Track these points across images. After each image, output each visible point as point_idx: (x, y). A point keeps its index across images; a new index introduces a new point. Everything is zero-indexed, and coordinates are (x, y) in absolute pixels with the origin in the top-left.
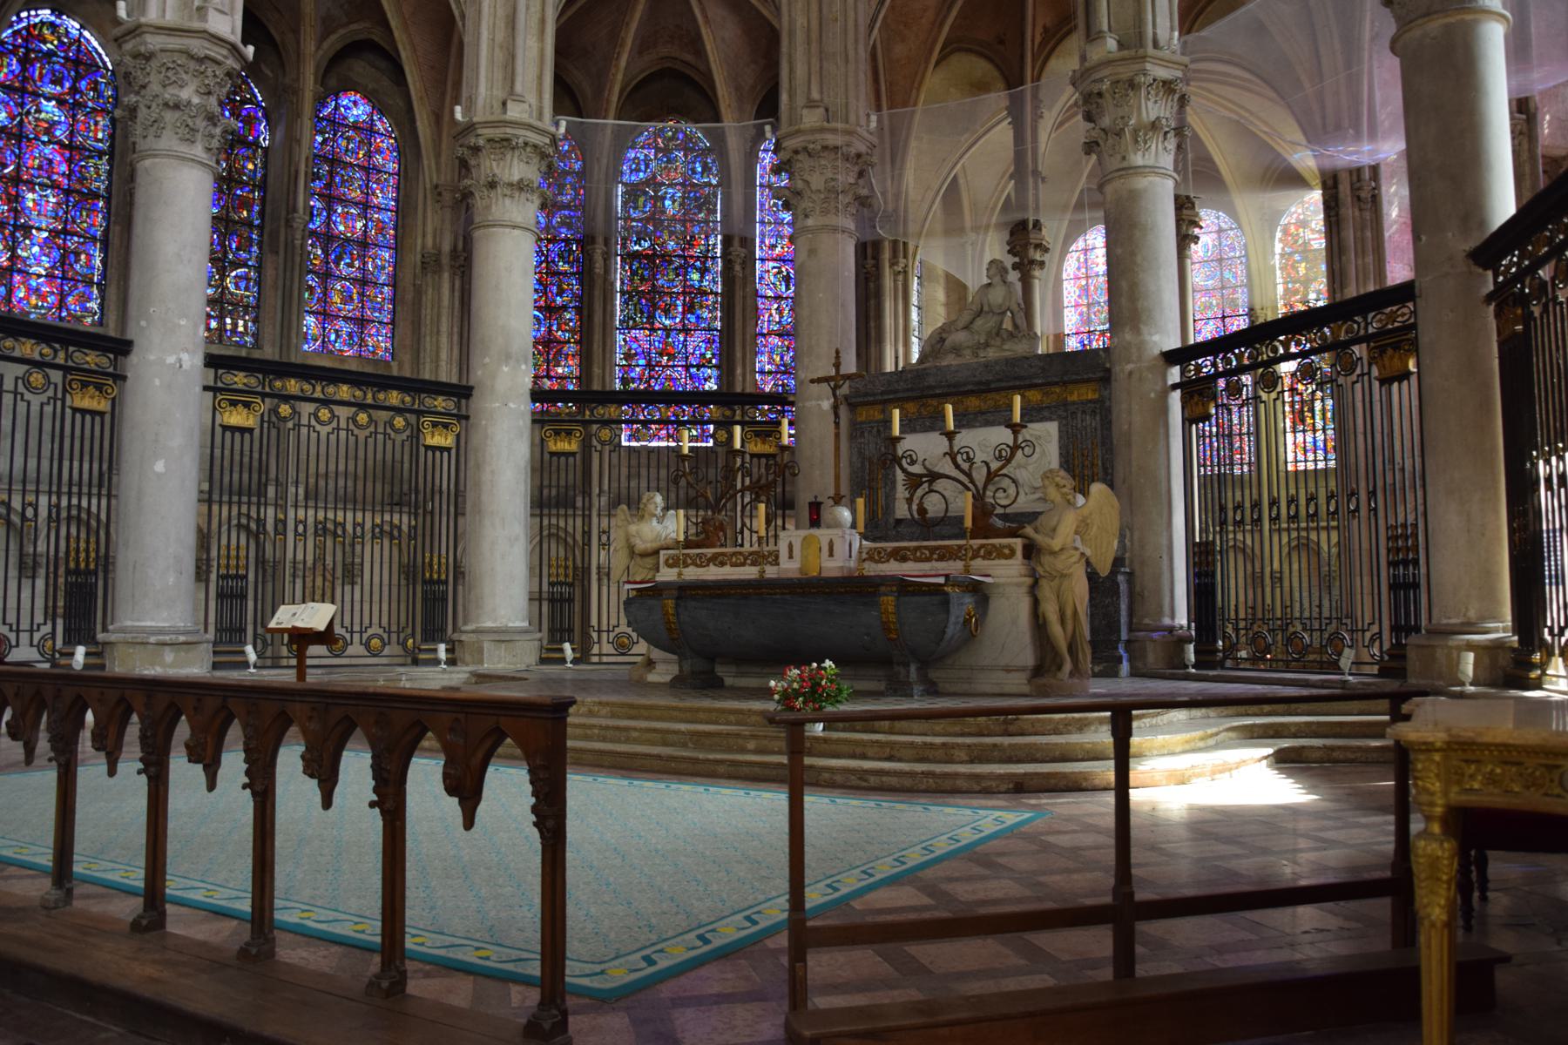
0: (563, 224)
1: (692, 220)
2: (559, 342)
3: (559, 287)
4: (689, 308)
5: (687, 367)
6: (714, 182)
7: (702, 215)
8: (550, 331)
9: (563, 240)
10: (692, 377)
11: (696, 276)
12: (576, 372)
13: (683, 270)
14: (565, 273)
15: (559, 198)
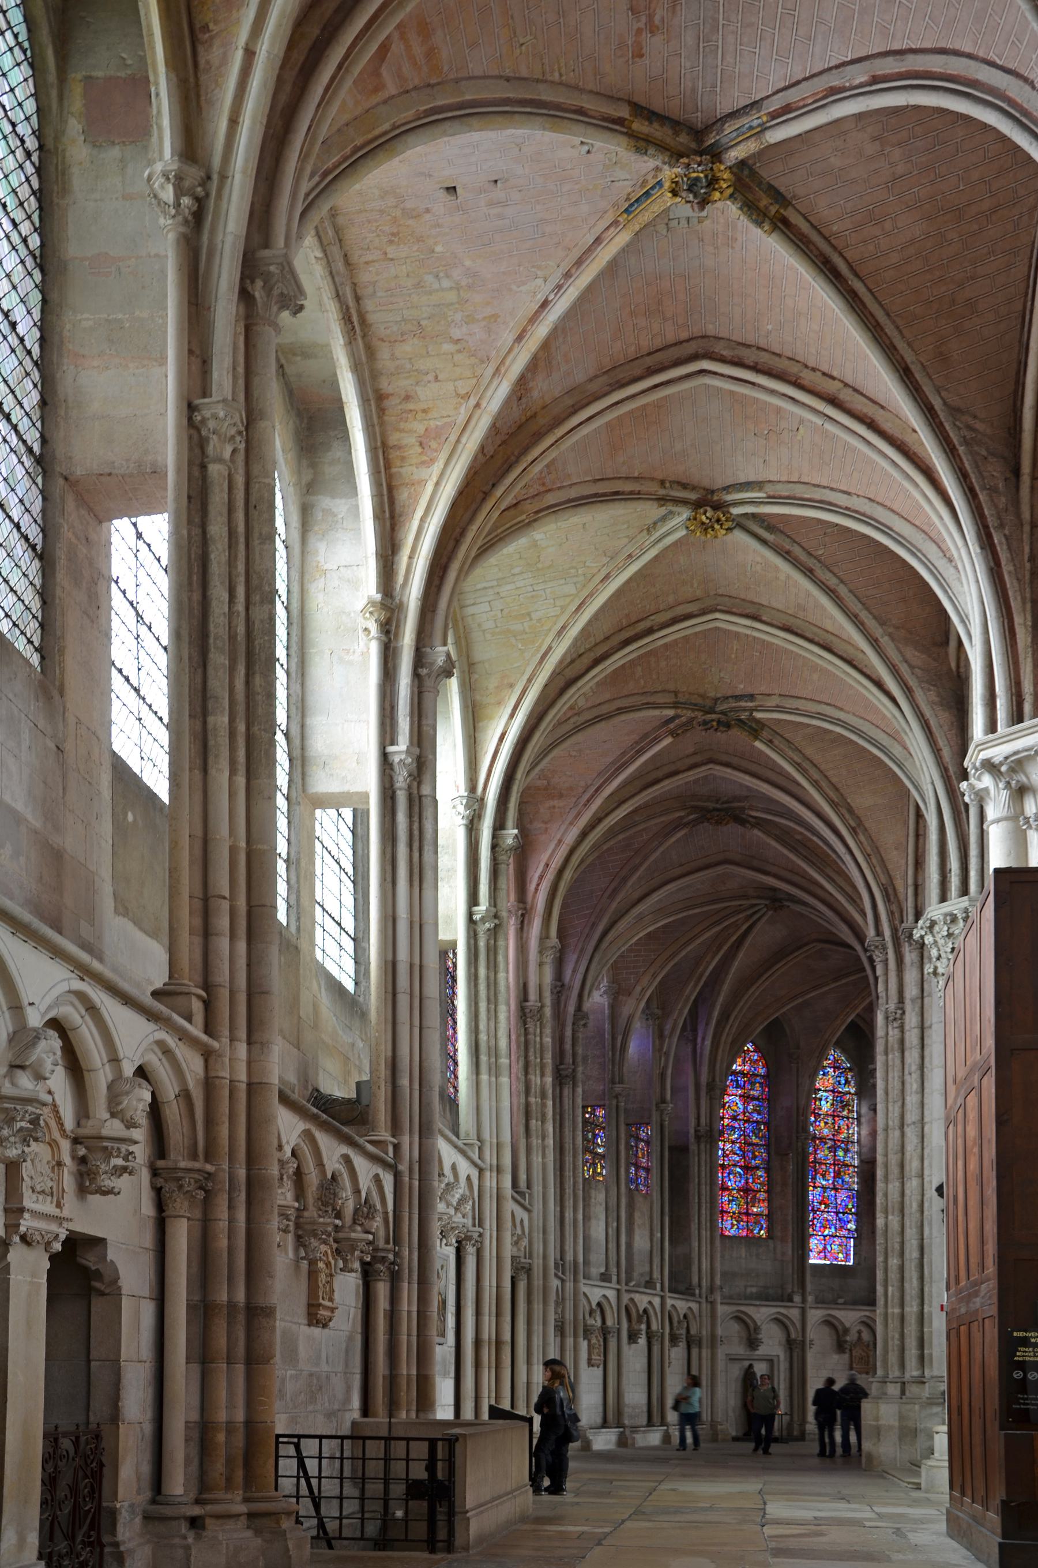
0: (754, 1110)
1: (838, 1116)
2: (753, 1191)
3: (753, 1153)
4: (837, 1175)
5: (837, 1213)
6: (853, 1091)
7: (845, 1113)
8: (747, 1182)
9: (754, 1122)
10: (840, 1220)
11: (841, 1153)
12: (766, 1212)
13: (833, 1149)
14: (757, 1145)
15: (752, 1092)
